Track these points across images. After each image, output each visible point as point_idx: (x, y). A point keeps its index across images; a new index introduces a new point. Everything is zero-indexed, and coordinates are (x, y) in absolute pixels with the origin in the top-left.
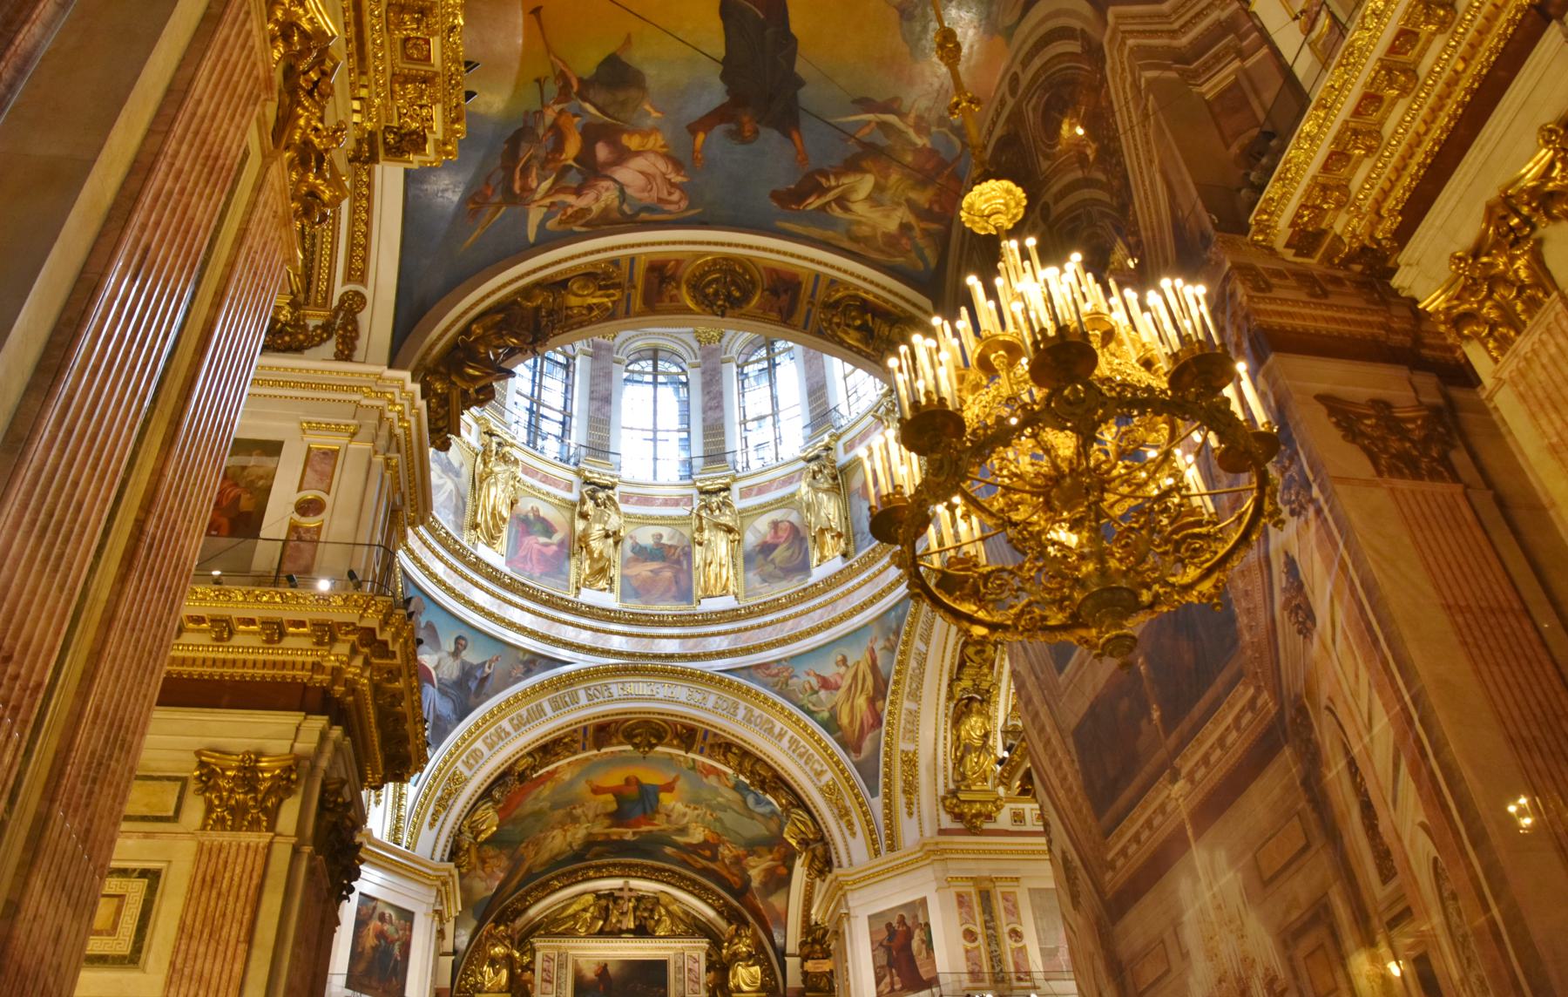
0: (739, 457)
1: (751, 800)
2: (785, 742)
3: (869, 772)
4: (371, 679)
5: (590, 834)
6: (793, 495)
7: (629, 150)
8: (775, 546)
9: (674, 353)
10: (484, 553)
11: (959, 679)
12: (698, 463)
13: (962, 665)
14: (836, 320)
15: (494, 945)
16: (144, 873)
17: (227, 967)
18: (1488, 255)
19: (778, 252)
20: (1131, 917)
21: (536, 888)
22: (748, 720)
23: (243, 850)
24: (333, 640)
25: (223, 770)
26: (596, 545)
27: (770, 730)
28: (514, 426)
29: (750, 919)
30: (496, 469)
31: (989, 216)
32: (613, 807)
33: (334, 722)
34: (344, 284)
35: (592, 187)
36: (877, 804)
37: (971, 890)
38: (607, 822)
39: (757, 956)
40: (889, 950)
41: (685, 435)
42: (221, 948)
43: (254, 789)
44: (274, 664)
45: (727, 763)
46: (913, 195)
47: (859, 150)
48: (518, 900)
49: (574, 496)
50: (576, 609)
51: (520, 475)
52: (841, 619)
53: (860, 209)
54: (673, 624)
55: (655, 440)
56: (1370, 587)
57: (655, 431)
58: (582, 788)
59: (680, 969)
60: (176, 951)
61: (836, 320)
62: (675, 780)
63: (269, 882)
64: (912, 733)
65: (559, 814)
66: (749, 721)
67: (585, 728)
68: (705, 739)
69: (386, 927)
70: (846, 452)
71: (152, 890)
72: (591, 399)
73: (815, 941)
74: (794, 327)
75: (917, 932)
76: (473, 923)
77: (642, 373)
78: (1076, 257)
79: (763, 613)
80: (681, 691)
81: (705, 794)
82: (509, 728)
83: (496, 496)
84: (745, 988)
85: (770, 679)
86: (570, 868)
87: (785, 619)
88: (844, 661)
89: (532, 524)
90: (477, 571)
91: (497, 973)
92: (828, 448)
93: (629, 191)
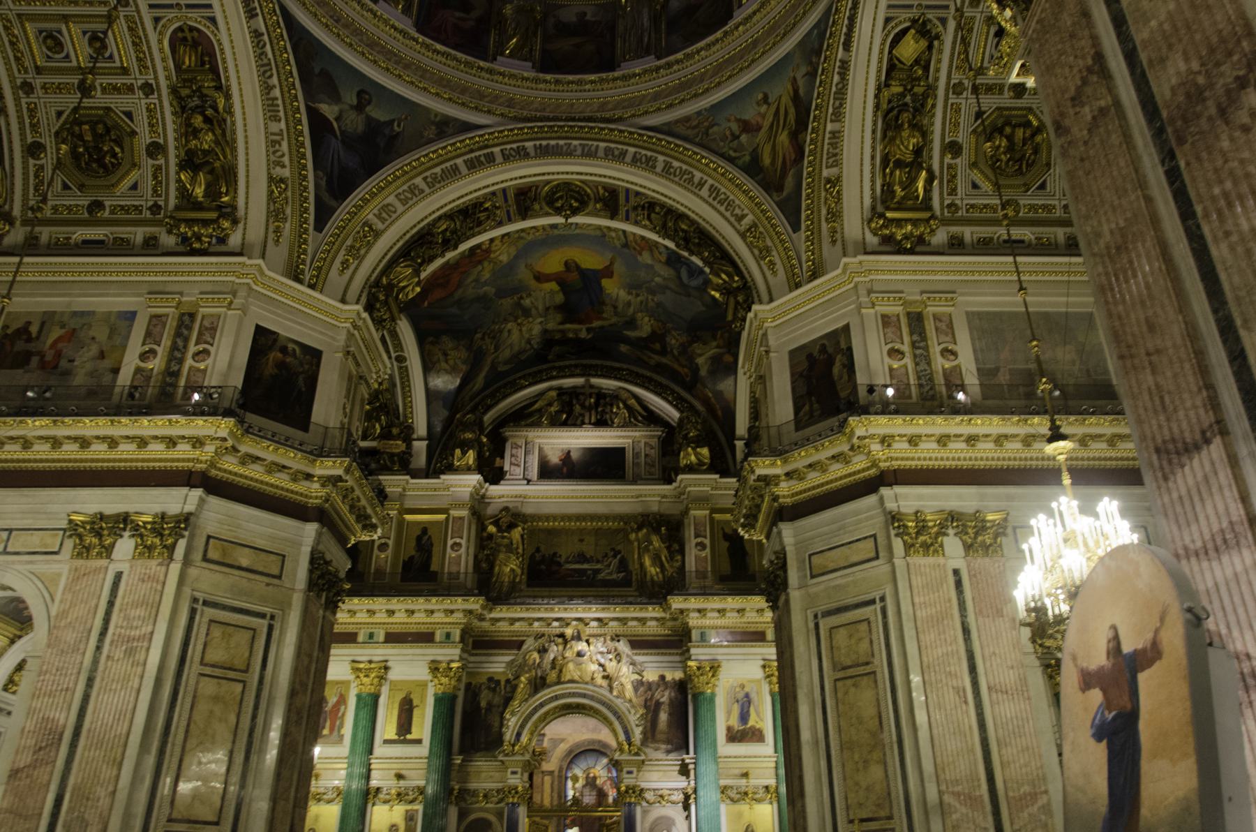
2: (705, 192)
5: (545, 331)
11: (887, 85)
13: (891, 68)
15: (464, 431)
27: (691, 180)
32: (560, 298)
38: (559, 317)
39: (706, 438)
45: (653, 230)
62: (612, 263)
65: (507, 303)
67: (504, 190)
68: (627, 200)
75: (839, 357)
76: (444, 413)
86: (535, 369)
88: (766, 99)
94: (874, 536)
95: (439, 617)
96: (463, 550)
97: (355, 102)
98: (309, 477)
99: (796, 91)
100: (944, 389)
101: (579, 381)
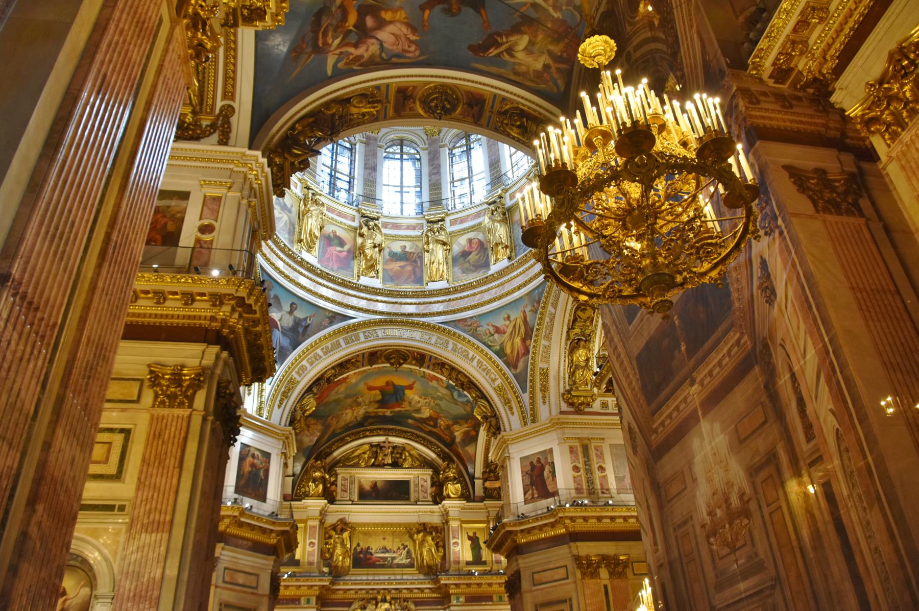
0: (450, 202)
1: (455, 394)
3: (521, 379)
4: (243, 325)
6: (480, 224)
7: (385, 20)
8: (470, 253)
9: (412, 141)
10: (306, 256)
11: (573, 328)
12: (426, 205)
13: (575, 320)
14: (505, 122)
16: (122, 431)
17: (169, 481)
18: (887, 83)
19: (472, 82)
20: (666, 458)
21: (337, 441)
22: (454, 350)
23: (175, 419)
24: (222, 304)
25: (163, 375)
26: (369, 252)
28: (321, 184)
29: (455, 459)
30: (312, 208)
31: (594, 57)
32: (379, 397)
33: (223, 349)
34: (222, 100)
35: (364, 43)
36: (526, 397)
37: (577, 444)
38: (376, 405)
39: (459, 479)
40: (531, 476)
41: (419, 189)
42: (165, 471)
43: (180, 385)
44: (189, 317)
45: (442, 374)
46: (551, 47)
47: (520, 20)
48: (327, 447)
49: (356, 224)
50: (357, 288)
51: (325, 212)
52: (507, 294)
53: (520, 56)
54: (412, 297)
55: (401, 192)
56: (808, 276)
57: (402, 186)
58: (362, 387)
59: (417, 485)
60: (141, 472)
61: (505, 122)
62: (414, 383)
63: (190, 436)
64: (546, 359)
65: (349, 401)
66: (455, 351)
67: (363, 354)
68: (430, 360)
69: (256, 461)
70: (511, 199)
71: (126, 440)
72: (365, 168)
73: (490, 471)
74: (481, 126)
76: (304, 460)
77: (394, 153)
78: (645, 81)
79: (463, 291)
80: (417, 334)
81: (430, 391)
82: (321, 353)
83: (312, 223)
84: (452, 496)
85: (467, 328)
87: (475, 294)
88: (508, 318)
89: (332, 240)
90: (302, 266)
91: (317, 486)
92: (500, 197)
93: (385, 45)
94: (566, 566)
95: (303, 591)
96: (316, 547)
97: (289, 309)
98: (272, 531)
99: (525, 318)
100: (600, 491)
101: (381, 439)
